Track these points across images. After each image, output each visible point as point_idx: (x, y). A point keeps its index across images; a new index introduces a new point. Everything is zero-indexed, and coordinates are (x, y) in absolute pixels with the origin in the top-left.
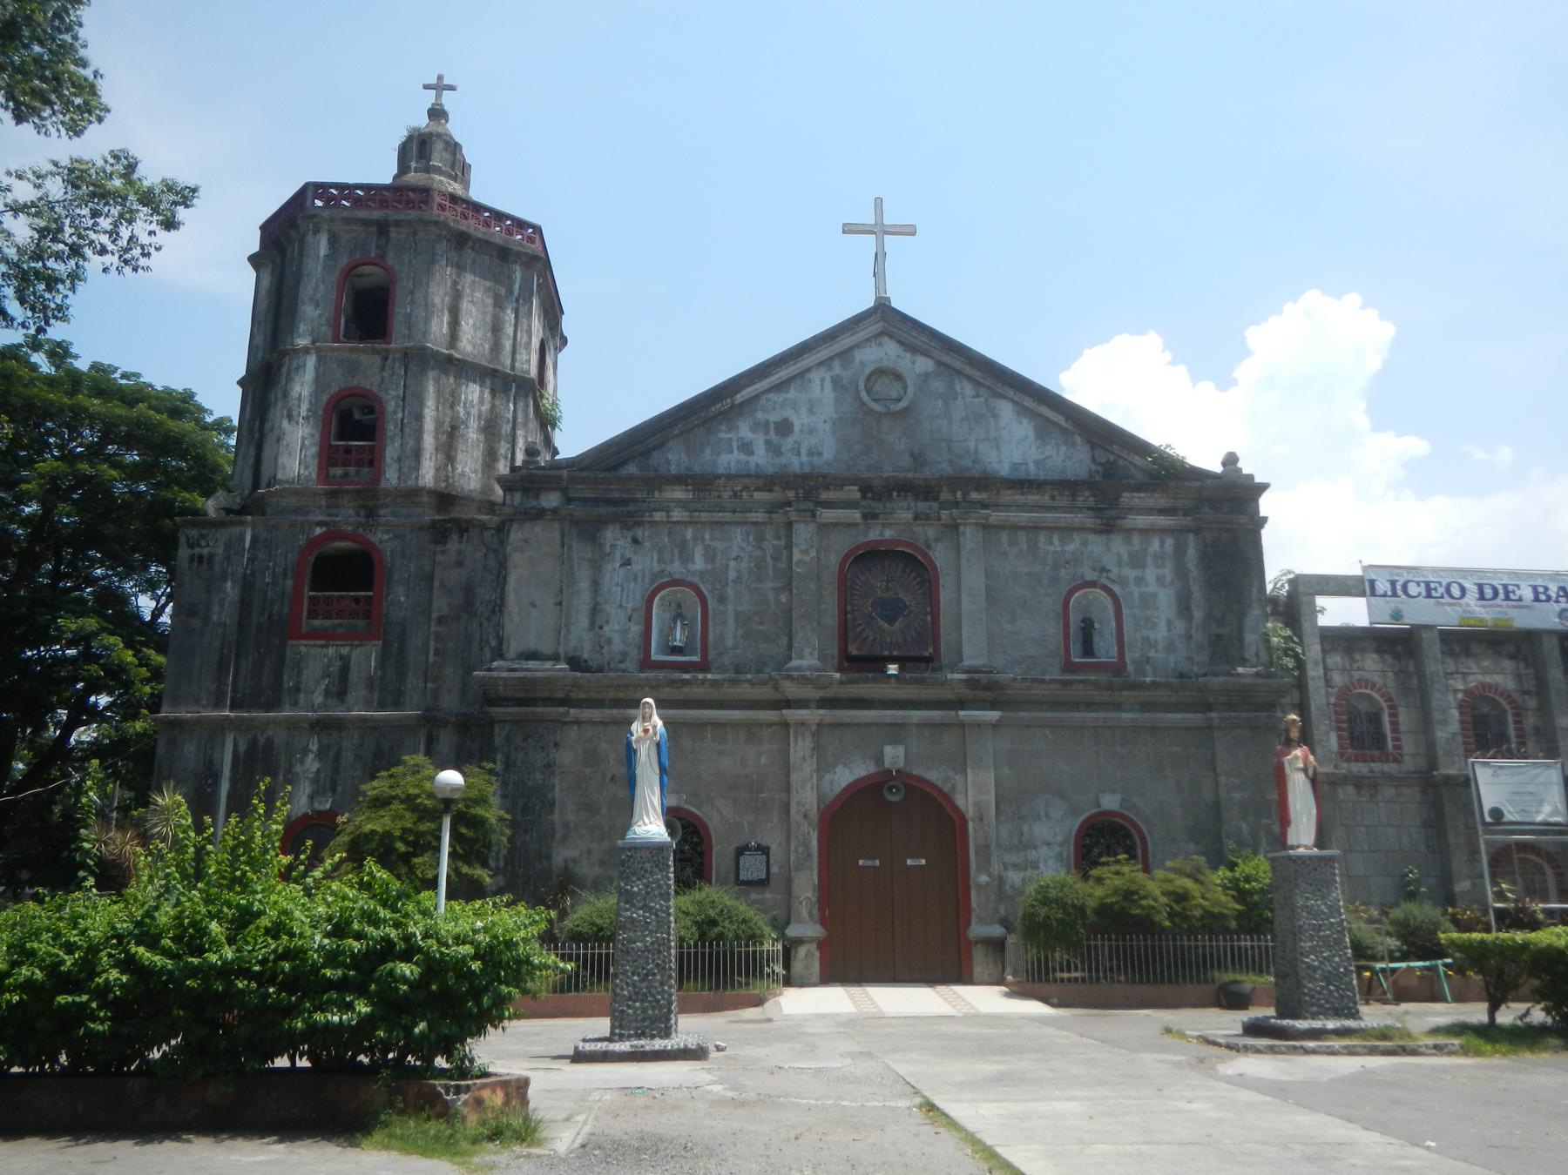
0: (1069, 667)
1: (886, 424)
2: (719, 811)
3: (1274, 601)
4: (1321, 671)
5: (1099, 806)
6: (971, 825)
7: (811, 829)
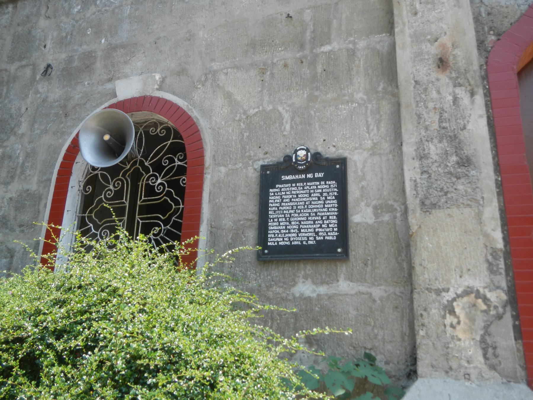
2: (228, 96)
7: (461, 92)
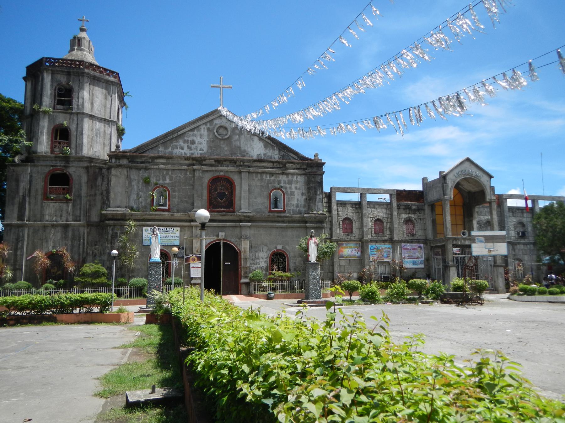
0: (270, 211)
1: (222, 142)
3: (326, 193)
4: (336, 212)
6: (242, 253)
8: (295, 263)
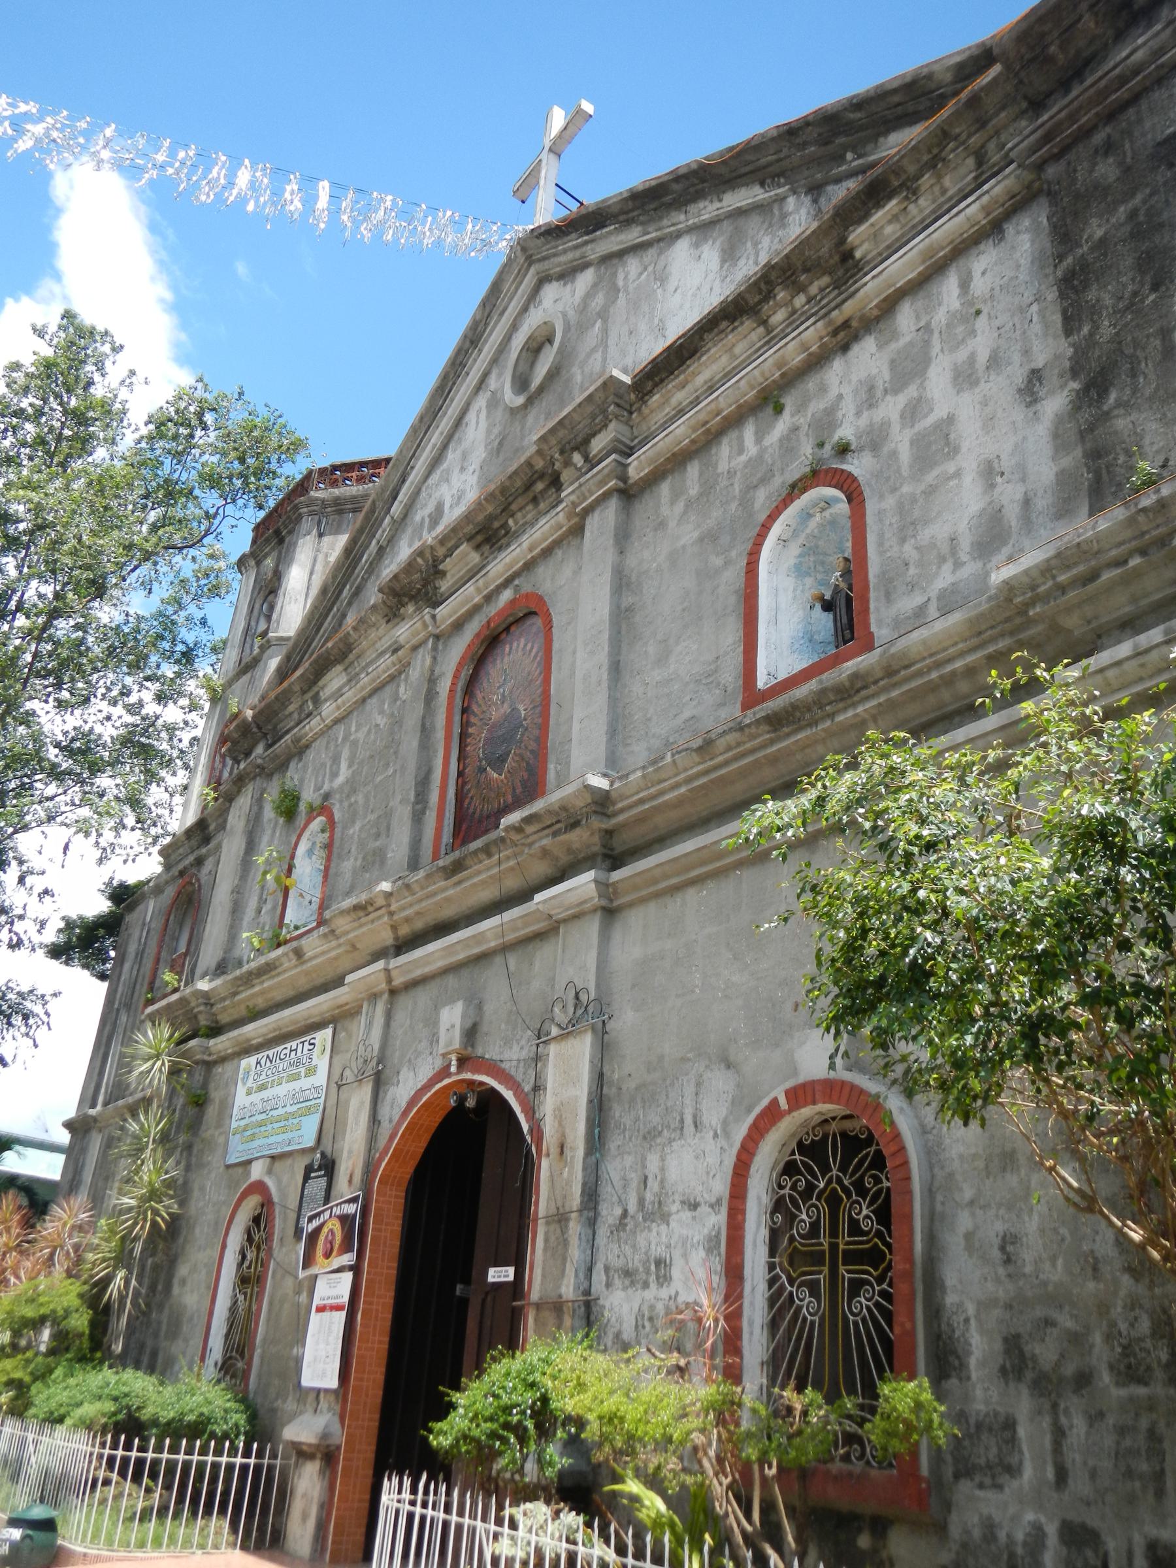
5: (795, 1072)
8: (1008, 1244)
